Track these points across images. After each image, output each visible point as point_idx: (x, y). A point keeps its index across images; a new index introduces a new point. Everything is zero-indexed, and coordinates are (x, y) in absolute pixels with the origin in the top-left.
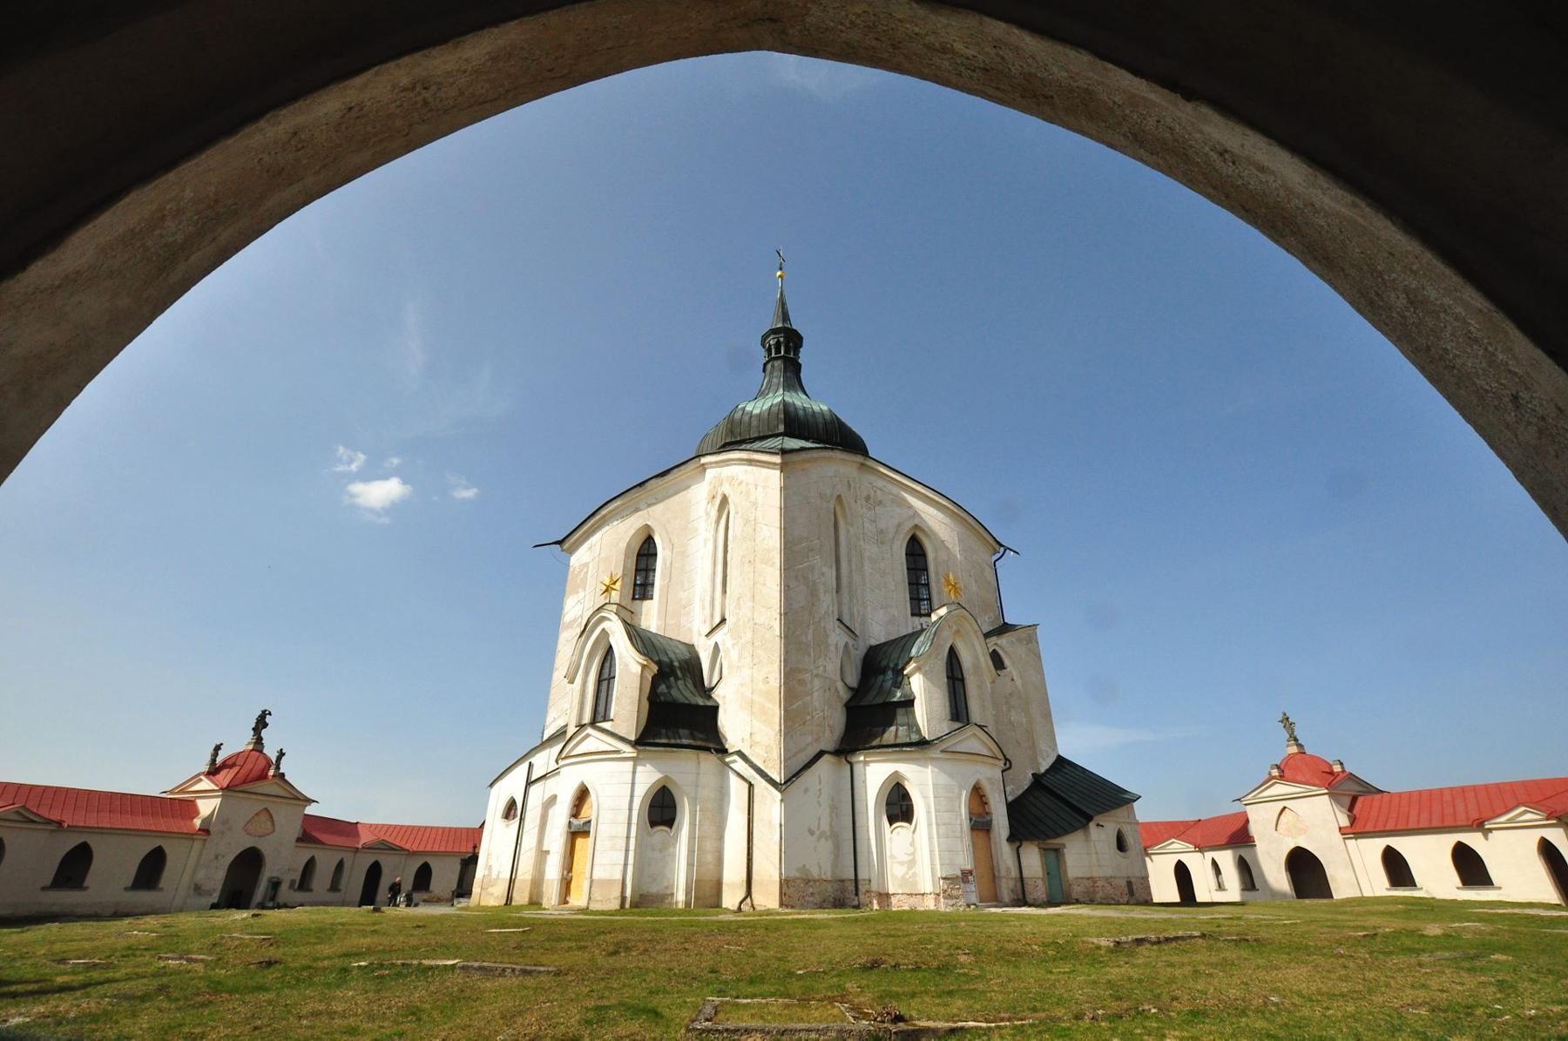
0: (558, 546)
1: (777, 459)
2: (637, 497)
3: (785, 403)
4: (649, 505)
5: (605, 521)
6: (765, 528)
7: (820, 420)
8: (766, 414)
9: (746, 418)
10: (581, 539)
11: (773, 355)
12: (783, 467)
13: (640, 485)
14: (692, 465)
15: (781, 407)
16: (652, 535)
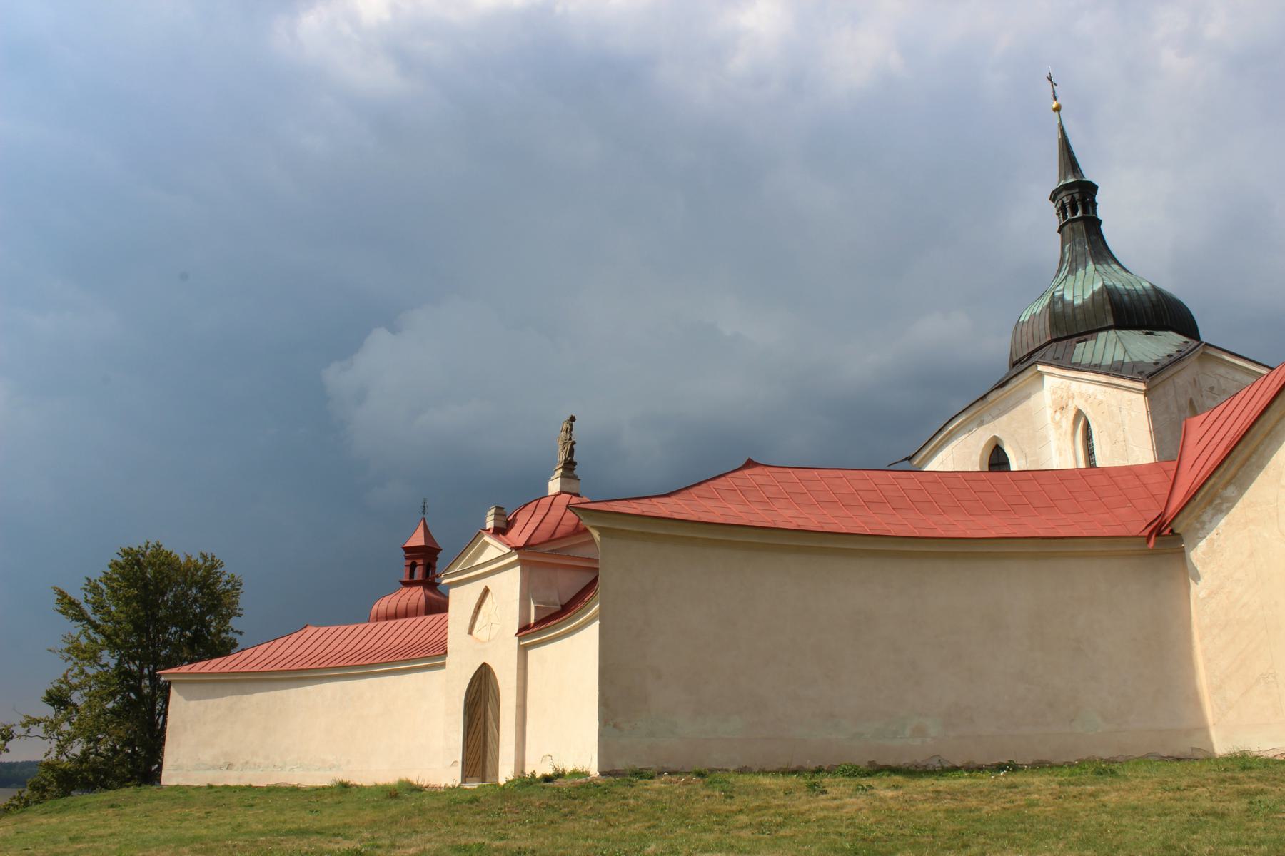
0: (907, 461)
1: (1142, 386)
2: (981, 409)
3: (1105, 286)
4: (994, 418)
5: (952, 436)
6: (1134, 448)
7: (1147, 304)
8: (1090, 305)
9: (1069, 310)
10: (929, 455)
11: (1069, 216)
12: (1146, 394)
13: (982, 398)
14: (1028, 373)
15: (1105, 295)
16: (1001, 445)
